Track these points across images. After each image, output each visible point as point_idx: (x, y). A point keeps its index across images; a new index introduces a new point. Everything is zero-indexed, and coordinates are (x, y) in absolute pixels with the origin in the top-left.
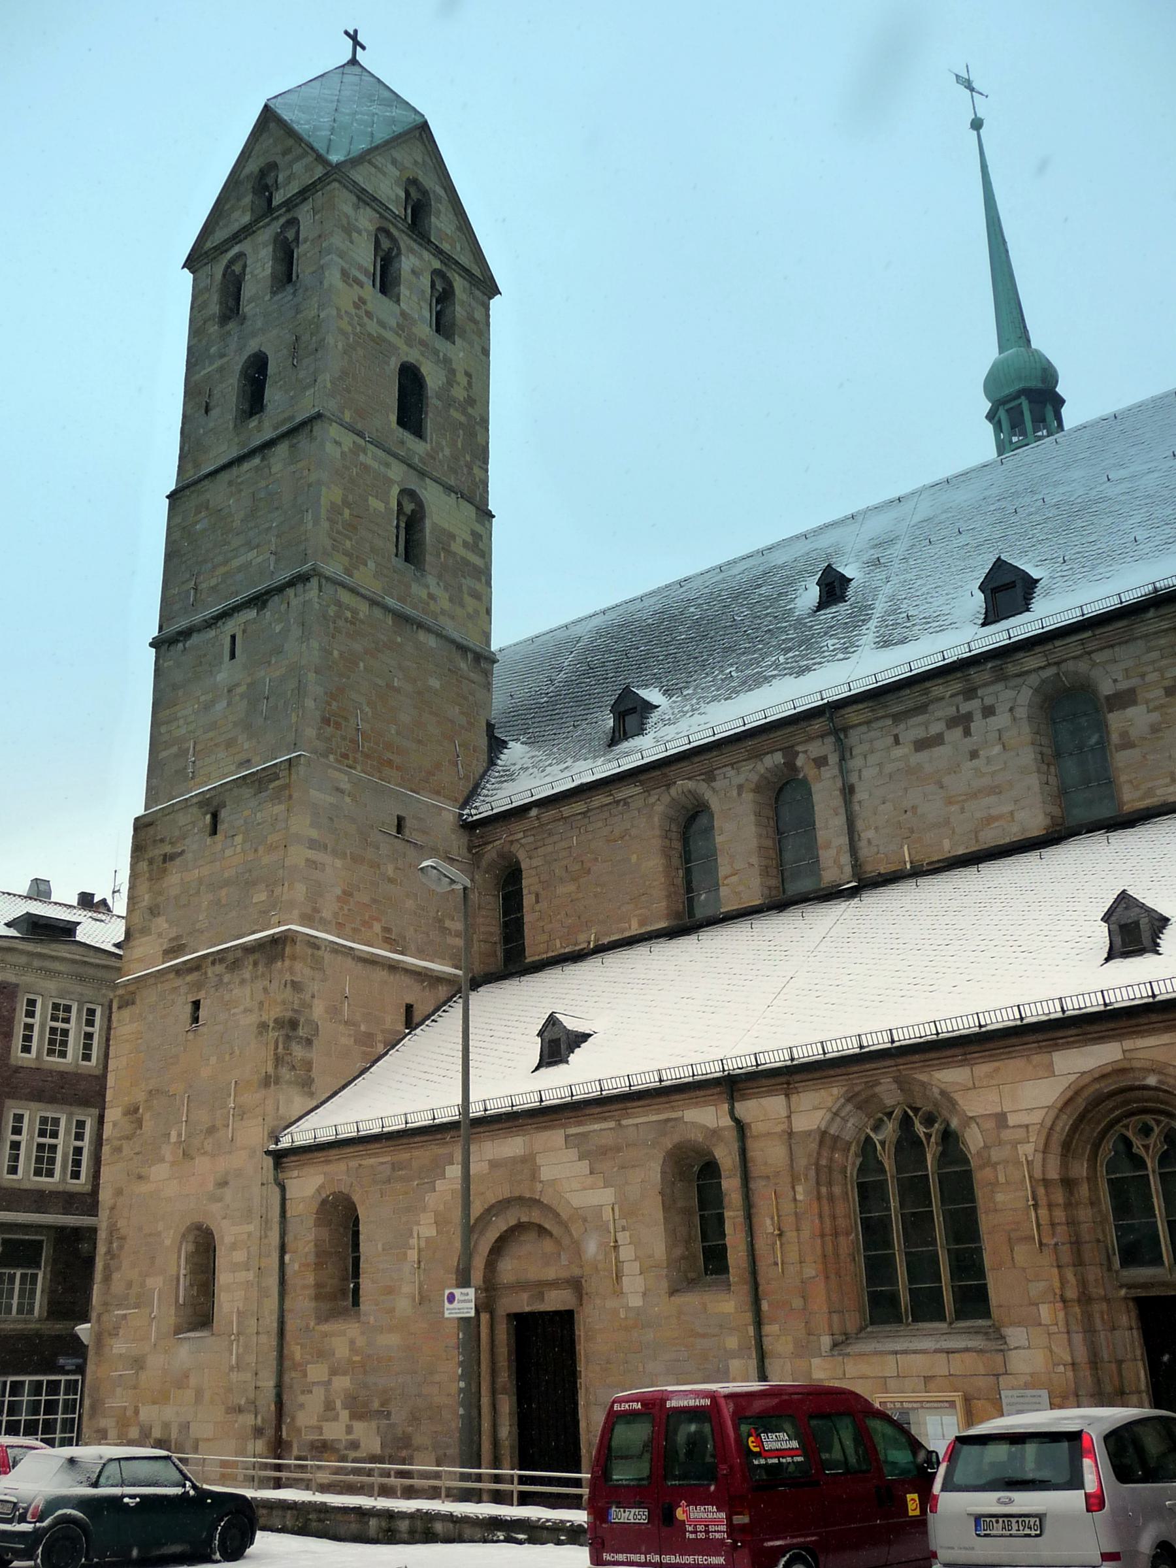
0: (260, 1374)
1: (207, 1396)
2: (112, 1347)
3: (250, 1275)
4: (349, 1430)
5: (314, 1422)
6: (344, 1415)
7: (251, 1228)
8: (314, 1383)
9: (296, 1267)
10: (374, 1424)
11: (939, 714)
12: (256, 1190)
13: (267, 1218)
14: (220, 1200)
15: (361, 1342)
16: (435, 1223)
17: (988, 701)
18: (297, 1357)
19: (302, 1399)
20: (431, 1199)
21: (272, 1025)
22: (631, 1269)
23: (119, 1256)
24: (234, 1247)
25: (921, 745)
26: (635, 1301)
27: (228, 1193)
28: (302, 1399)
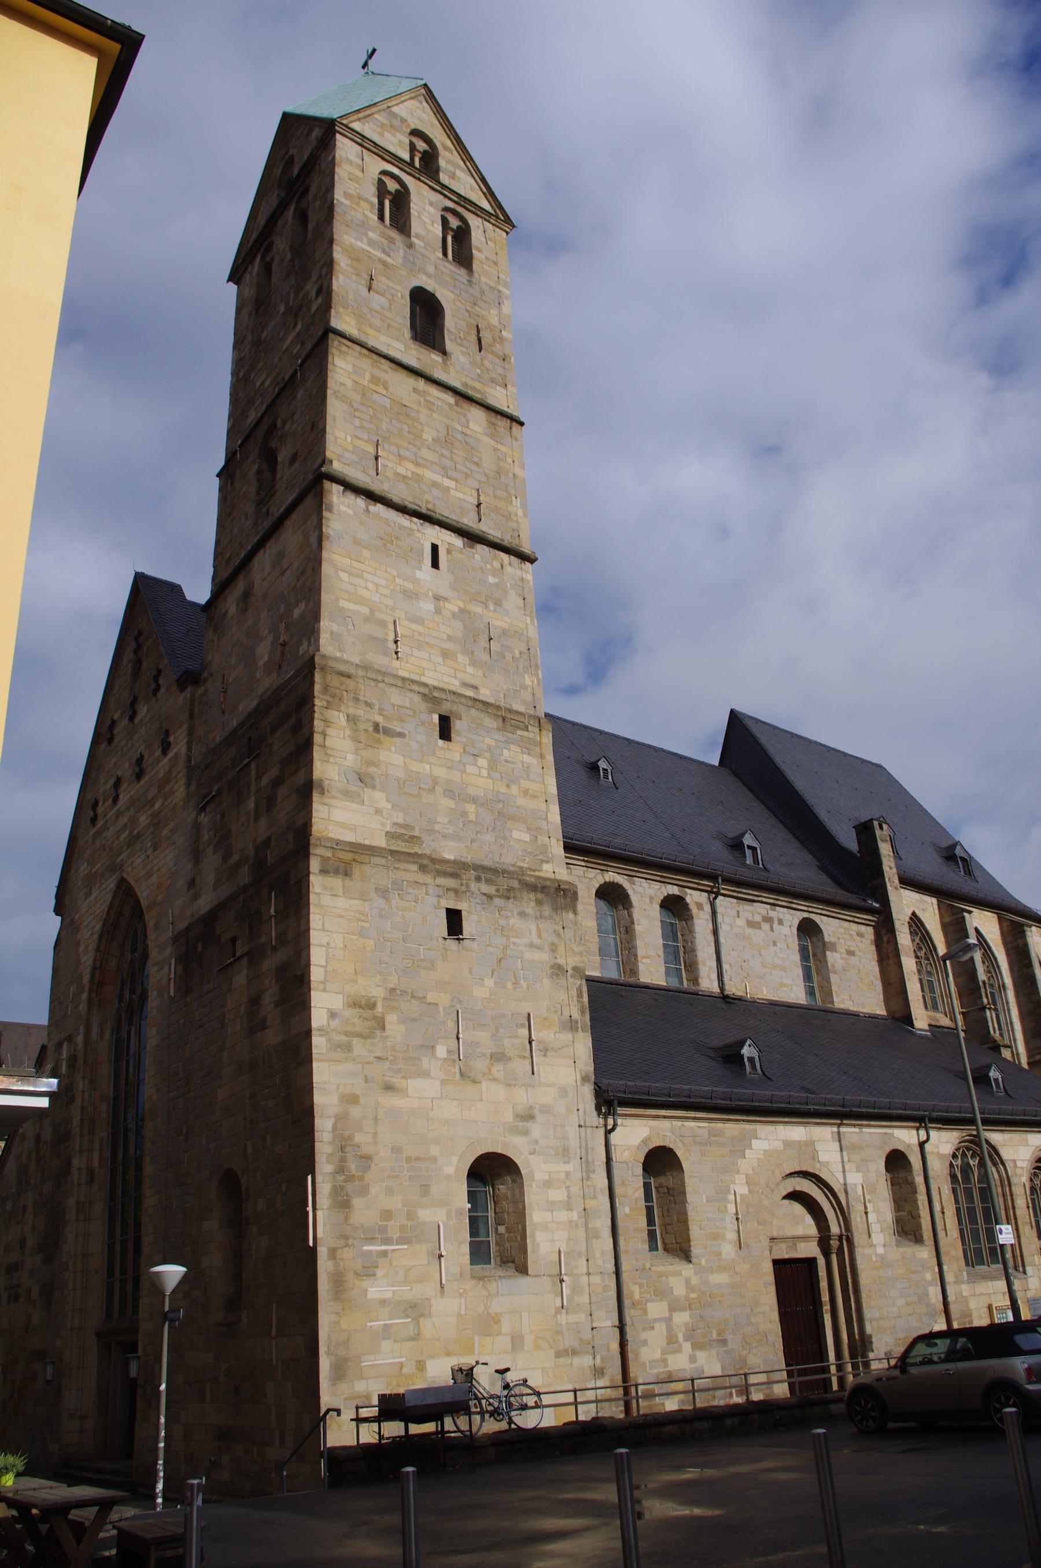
0: (596, 1315)
1: (529, 1340)
2: (366, 1290)
3: (574, 1216)
4: (693, 1359)
5: (657, 1355)
6: (687, 1346)
7: (569, 1167)
8: (655, 1320)
9: (627, 1210)
10: (714, 1352)
11: (759, 910)
12: (572, 1131)
13: (587, 1161)
14: (526, 1133)
15: (695, 1281)
16: (747, 1183)
17: (781, 916)
18: (637, 1296)
19: (644, 1335)
20: (743, 1165)
21: (570, 972)
22: (875, 1228)
23: (361, 1178)
24: (548, 1184)
25: (751, 924)
26: (880, 1250)
27: (536, 1130)
28: (644, 1335)
